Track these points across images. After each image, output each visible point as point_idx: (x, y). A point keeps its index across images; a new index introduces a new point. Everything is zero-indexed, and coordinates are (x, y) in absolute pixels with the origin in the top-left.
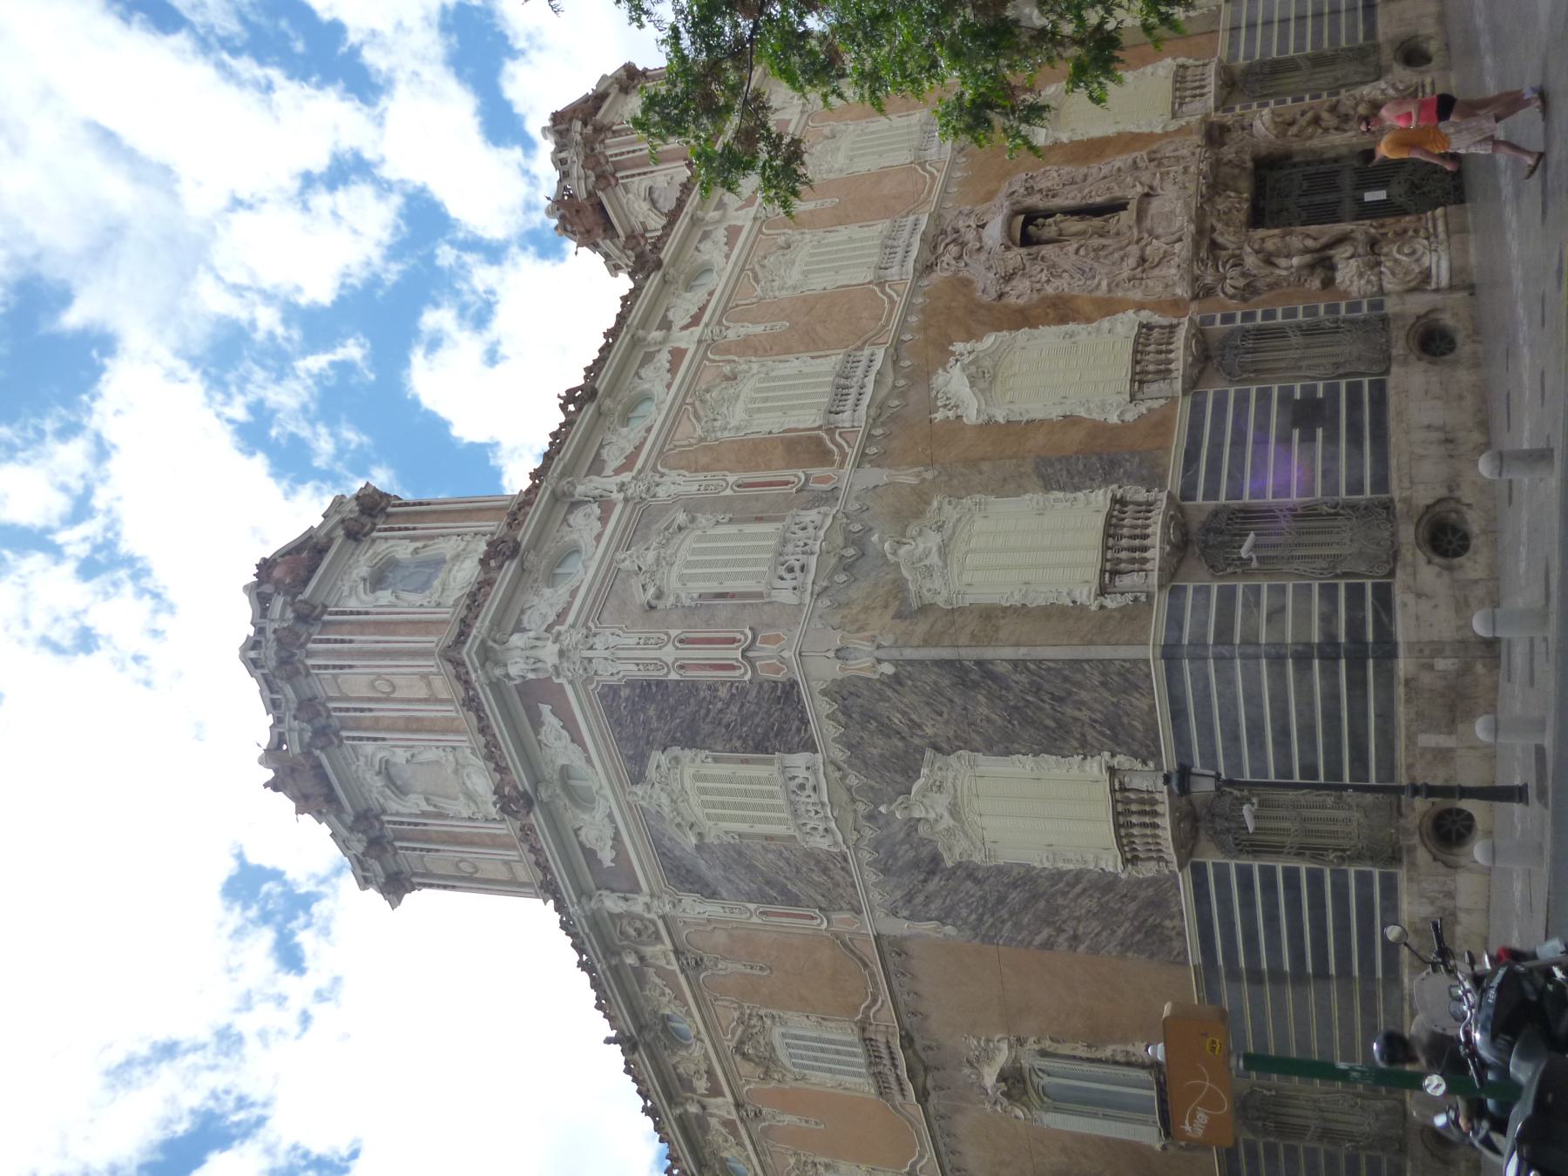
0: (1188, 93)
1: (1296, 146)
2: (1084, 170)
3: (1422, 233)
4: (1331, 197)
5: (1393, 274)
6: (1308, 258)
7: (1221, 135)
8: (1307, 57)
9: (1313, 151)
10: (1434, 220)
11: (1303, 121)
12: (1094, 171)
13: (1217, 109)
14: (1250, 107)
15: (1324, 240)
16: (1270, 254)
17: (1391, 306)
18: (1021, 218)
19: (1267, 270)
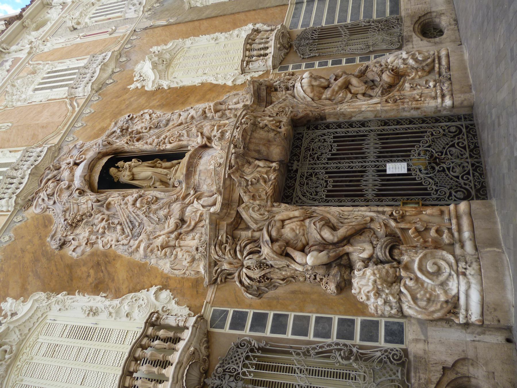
0: (255, 53)
1: (328, 110)
2: (168, 115)
3: (446, 238)
4: (357, 165)
5: (415, 299)
6: (323, 257)
7: (268, 94)
8: (346, 26)
9: (343, 114)
10: (458, 217)
11: (336, 85)
12: (175, 117)
13: (274, 67)
14: (300, 67)
15: (342, 232)
16: (288, 244)
17: (413, 342)
18: (105, 160)
19: (282, 262)
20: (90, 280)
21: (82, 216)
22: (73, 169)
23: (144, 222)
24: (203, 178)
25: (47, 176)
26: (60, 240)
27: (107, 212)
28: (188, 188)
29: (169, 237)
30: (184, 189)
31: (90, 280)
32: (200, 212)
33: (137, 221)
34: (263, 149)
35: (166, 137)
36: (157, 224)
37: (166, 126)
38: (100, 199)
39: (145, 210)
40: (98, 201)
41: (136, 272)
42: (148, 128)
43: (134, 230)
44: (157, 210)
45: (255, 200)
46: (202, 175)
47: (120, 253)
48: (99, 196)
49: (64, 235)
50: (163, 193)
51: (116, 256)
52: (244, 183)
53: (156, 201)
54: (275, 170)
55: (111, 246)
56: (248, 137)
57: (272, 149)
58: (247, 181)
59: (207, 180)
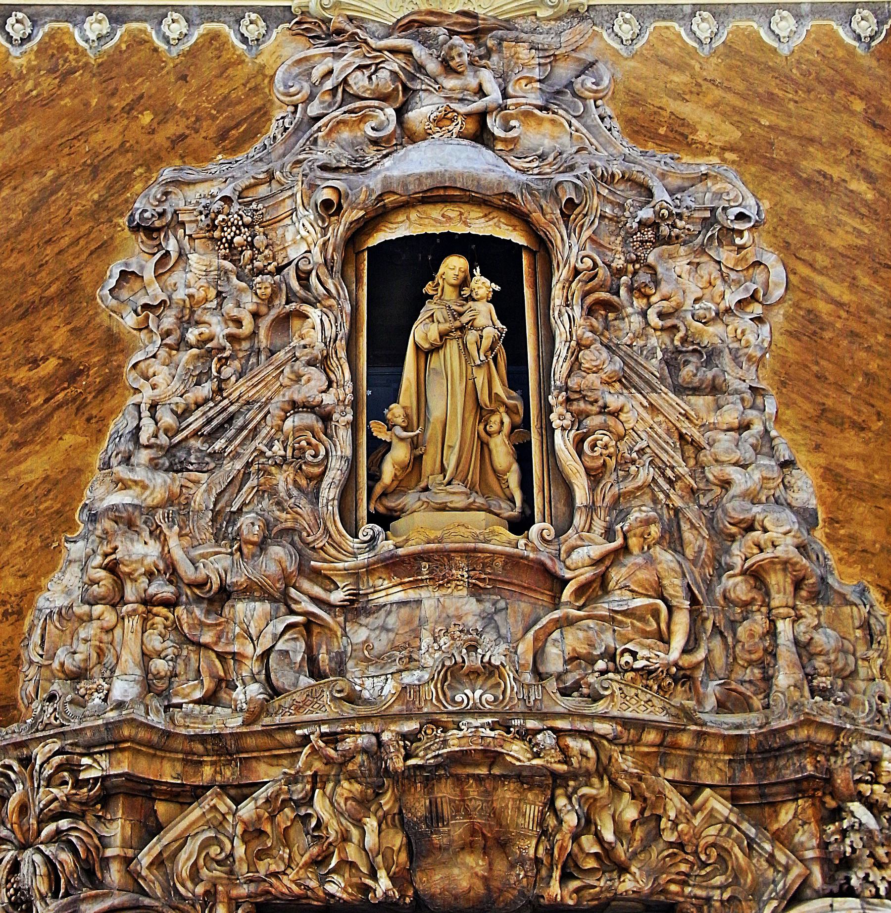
20: (22, 375)
21: (251, 245)
22: (452, 120)
23: (227, 466)
24: (391, 621)
25: (425, 41)
26: (162, 215)
27: (264, 324)
28: (355, 575)
29: (150, 575)
30: (350, 563)
31: (22, 375)
32: (249, 649)
33: (230, 441)
34: (456, 830)
35: (616, 414)
36: (216, 515)
37: (680, 390)
38: (313, 279)
39: (269, 453)
40: (303, 278)
41: (42, 507)
42: (669, 322)
43: (196, 443)
44: (273, 492)
45: (245, 842)
46: (405, 611)
47: (112, 428)
48: (323, 271)
49: (182, 218)
50: (334, 493)
51: (103, 419)
52: (299, 790)
53: (309, 478)
54: (367, 889)
55: (137, 391)
56: (483, 771)
57: (470, 860)
58: (309, 801)
59: (384, 636)
